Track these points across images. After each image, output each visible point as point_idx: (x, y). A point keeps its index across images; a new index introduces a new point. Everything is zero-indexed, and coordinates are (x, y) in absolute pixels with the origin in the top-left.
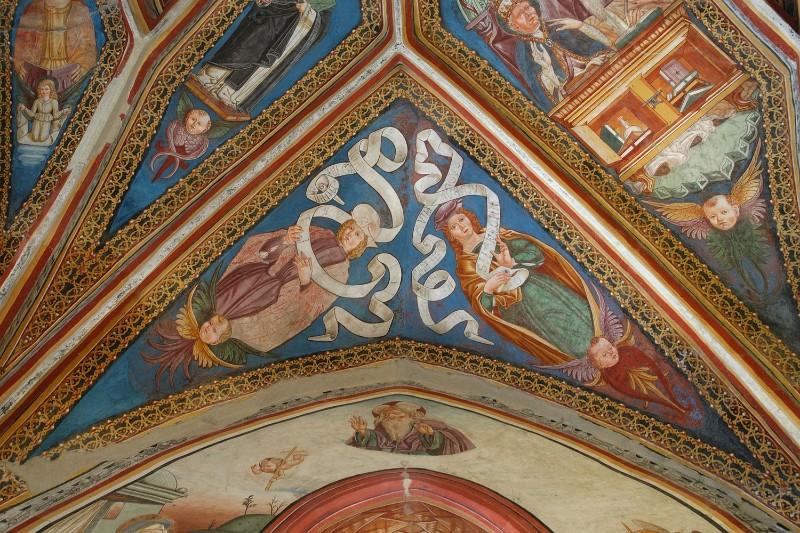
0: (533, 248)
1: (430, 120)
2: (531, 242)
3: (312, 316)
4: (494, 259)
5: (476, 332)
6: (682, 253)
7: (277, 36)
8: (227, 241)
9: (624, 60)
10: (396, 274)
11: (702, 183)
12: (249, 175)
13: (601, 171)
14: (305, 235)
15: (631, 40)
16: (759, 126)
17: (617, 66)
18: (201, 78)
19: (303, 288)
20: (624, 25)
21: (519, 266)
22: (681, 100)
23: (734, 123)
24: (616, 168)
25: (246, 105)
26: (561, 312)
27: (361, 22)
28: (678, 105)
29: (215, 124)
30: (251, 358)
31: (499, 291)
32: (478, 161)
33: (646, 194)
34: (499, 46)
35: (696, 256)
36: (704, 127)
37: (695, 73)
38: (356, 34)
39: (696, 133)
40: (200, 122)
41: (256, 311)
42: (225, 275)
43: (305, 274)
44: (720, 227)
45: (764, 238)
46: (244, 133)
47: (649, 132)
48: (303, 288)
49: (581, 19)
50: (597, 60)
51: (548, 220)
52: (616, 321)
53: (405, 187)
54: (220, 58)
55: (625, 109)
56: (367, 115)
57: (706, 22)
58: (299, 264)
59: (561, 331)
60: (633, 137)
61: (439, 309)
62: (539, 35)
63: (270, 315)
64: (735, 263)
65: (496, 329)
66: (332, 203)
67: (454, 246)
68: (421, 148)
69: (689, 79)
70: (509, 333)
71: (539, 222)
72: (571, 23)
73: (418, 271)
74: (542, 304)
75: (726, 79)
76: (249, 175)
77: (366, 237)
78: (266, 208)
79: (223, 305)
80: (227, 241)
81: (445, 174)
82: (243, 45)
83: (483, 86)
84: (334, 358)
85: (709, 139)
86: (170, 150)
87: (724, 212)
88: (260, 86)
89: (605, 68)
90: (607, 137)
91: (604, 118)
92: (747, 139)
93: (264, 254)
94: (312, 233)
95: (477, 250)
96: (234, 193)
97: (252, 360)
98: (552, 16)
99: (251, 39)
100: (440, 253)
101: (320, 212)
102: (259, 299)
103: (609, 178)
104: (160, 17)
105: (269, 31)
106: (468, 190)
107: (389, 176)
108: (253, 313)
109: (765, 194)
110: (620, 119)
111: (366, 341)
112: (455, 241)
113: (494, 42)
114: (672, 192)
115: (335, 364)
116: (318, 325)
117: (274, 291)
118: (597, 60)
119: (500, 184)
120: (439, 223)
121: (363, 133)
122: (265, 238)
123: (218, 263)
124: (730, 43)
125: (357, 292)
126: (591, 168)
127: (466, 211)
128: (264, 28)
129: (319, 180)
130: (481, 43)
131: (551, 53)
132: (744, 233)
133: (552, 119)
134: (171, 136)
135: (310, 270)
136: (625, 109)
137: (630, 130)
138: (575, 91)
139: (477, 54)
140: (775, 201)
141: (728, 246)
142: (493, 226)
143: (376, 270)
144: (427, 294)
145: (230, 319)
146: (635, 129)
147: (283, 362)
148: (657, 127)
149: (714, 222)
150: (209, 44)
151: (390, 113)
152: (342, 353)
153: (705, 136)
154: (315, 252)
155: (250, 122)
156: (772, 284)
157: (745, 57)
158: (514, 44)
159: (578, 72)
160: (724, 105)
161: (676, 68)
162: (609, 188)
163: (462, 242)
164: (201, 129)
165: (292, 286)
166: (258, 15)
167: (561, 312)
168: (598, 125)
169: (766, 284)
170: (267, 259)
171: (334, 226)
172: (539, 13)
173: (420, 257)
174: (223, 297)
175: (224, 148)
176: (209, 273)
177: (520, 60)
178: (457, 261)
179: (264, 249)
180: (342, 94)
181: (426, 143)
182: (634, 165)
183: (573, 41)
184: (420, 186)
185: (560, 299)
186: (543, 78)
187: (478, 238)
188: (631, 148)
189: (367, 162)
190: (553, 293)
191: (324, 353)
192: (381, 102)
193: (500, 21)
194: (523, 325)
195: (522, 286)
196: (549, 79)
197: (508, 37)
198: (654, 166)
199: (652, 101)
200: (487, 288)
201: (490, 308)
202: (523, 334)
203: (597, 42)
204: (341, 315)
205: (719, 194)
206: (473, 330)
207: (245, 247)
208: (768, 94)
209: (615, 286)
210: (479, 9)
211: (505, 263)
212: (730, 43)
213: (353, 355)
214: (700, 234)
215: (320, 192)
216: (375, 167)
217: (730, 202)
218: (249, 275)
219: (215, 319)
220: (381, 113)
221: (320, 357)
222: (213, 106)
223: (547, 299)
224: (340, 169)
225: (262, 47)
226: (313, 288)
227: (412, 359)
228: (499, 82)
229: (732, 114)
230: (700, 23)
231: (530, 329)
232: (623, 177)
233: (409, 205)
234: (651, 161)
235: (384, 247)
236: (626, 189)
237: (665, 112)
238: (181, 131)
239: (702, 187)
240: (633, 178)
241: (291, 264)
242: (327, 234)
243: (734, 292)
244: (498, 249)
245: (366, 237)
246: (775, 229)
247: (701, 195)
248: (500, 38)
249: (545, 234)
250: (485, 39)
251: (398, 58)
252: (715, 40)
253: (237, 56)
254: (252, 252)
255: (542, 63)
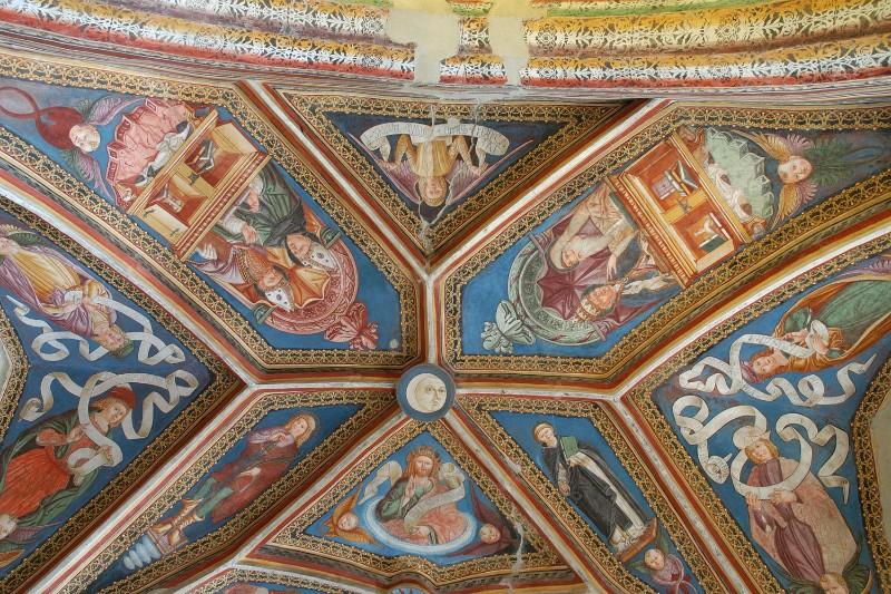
0: (795, 315)
1: (672, 376)
2: (789, 315)
3: (825, 497)
4: (798, 344)
5: (860, 365)
6: (827, 207)
7: (593, 485)
8: (755, 558)
9: (648, 225)
10: (794, 418)
11: (764, 180)
12: (706, 536)
13: (740, 256)
14: (754, 490)
15: (632, 218)
16: (720, 129)
17: (652, 231)
18: (620, 549)
19: (799, 500)
20: (620, 222)
21: (809, 327)
22: (688, 186)
23: (714, 148)
24: (737, 244)
25: (645, 520)
26: (859, 302)
27: (589, 419)
28: (691, 189)
29: (658, 547)
30: (861, 561)
31: (827, 344)
32: (716, 346)
33: (767, 225)
34: (622, 318)
35: (833, 196)
36: (714, 172)
37: (666, 173)
38: (597, 424)
39: (718, 179)
40: (654, 557)
41: (818, 547)
42: (784, 566)
43: (787, 497)
44: (808, 172)
45: (826, 141)
46: (667, 525)
47: (712, 214)
48: (799, 500)
49: (610, 254)
50: (645, 246)
51: (773, 301)
52: (880, 264)
53: (723, 401)
54: (606, 531)
55: (689, 230)
56: (662, 425)
57: (626, 160)
58: (778, 500)
59: (878, 304)
60: (714, 227)
61: (832, 388)
62: (617, 287)
63: (822, 534)
64: (846, 167)
65: (860, 351)
66: (729, 463)
67: (779, 371)
68: (693, 385)
69: (670, 178)
70: (868, 342)
71: (774, 307)
72: (612, 262)
73: (795, 400)
74: (848, 314)
75: (675, 149)
76: (706, 536)
77: (761, 440)
78: (729, 519)
79: (811, 576)
80: (755, 558)
81: (718, 371)
82: (597, 511)
83: (651, 334)
84: (865, 483)
85: (725, 169)
86: (675, 585)
87: (794, 168)
88: (630, 505)
89: (652, 241)
90: (711, 247)
91: (693, 246)
92: (730, 140)
93: (768, 528)
94: (753, 484)
95: (787, 355)
96: (720, 551)
97: (864, 560)
98: (604, 276)
99: (594, 504)
100: (784, 383)
101: (736, 475)
102: (807, 541)
103: (747, 251)
104: (570, 570)
105: (589, 491)
106: (735, 355)
107: (713, 413)
108: (820, 549)
109: (783, 134)
110: (696, 234)
111: (852, 454)
112: (776, 370)
113: (618, 322)
114: (768, 204)
115: (871, 484)
116: (834, 493)
117: (800, 526)
118: (645, 246)
119: (734, 331)
120: (758, 380)
121: (676, 430)
122: (754, 525)
123: (773, 570)
124: (645, 143)
125: (807, 454)
126: (736, 263)
127: (752, 359)
128: (585, 493)
129: (710, 471)
130: (618, 332)
131: (633, 280)
132: (817, 156)
133: (688, 286)
134: (663, 582)
135: (784, 491)
136: (689, 230)
137: (707, 228)
138: (667, 265)
139: (626, 335)
140: (791, 127)
141: (827, 169)
142: (768, 341)
143: (789, 435)
144: (817, 397)
145: (824, 572)
146: (707, 225)
147: (867, 532)
148: (707, 208)
149: (802, 177)
150: (594, 537)
151: (662, 406)
152: (861, 476)
153: (721, 172)
154: (769, 484)
155: (658, 519)
156: (877, 143)
157: (658, 133)
158: (622, 307)
159: (652, 261)
160: (697, 154)
161: (659, 187)
162: (755, 253)
163: (777, 366)
164: (660, 558)
165: (797, 509)
166: (577, 496)
167: (859, 302)
168: (699, 252)
169: (873, 147)
170: (771, 525)
171: (749, 465)
172: (599, 286)
173: (784, 398)
174: (803, 572)
175: (677, 543)
176: (782, 580)
177: (636, 304)
178: (794, 371)
179: (763, 528)
180: (648, 448)
181: (689, 381)
182: (739, 230)
183: (627, 262)
184: (724, 390)
185: (845, 301)
186: (653, 288)
187: (777, 354)
188: (723, 230)
189: (699, 430)
190: (839, 305)
191: (860, 492)
192: (653, 412)
193: (602, 315)
194: (864, 330)
195: (827, 326)
196: (654, 284)
197: (616, 311)
198: (742, 215)
199: (685, 209)
200: (821, 352)
201: (841, 352)
202: (875, 329)
203: (630, 244)
204: (826, 472)
205: (776, 170)
206: (856, 368)
207: (761, 543)
208: (693, 119)
209: (846, 260)
210: (590, 329)
211: (804, 337)
212: (645, 143)
213: (864, 466)
214: (811, 190)
215: (719, 472)
216: (704, 424)
217: (785, 162)
218: (785, 546)
219: (824, 585)
220: (661, 414)
221: (863, 496)
222: (645, 543)
223: (844, 310)
224: (703, 453)
225: (600, 497)
226: (799, 492)
227: (874, 415)
228: (651, 322)
229: (706, 149)
230: (626, 165)
231: (869, 325)
232: (748, 240)
233: (737, 399)
234: (736, 215)
235: (771, 426)
236: (759, 239)
237: (696, 200)
238: (661, 574)
239: (768, 181)
240: (750, 233)
241: (778, 507)
242: (757, 472)
243: (877, 174)
244: (789, 340)
245: (761, 440)
246: (819, 131)
247: (775, 183)
248: (616, 317)
249: (784, 306)
250: (615, 327)
251: (624, 400)
252: (641, 154)
253: (606, 518)
254: (766, 538)
255: (640, 288)
